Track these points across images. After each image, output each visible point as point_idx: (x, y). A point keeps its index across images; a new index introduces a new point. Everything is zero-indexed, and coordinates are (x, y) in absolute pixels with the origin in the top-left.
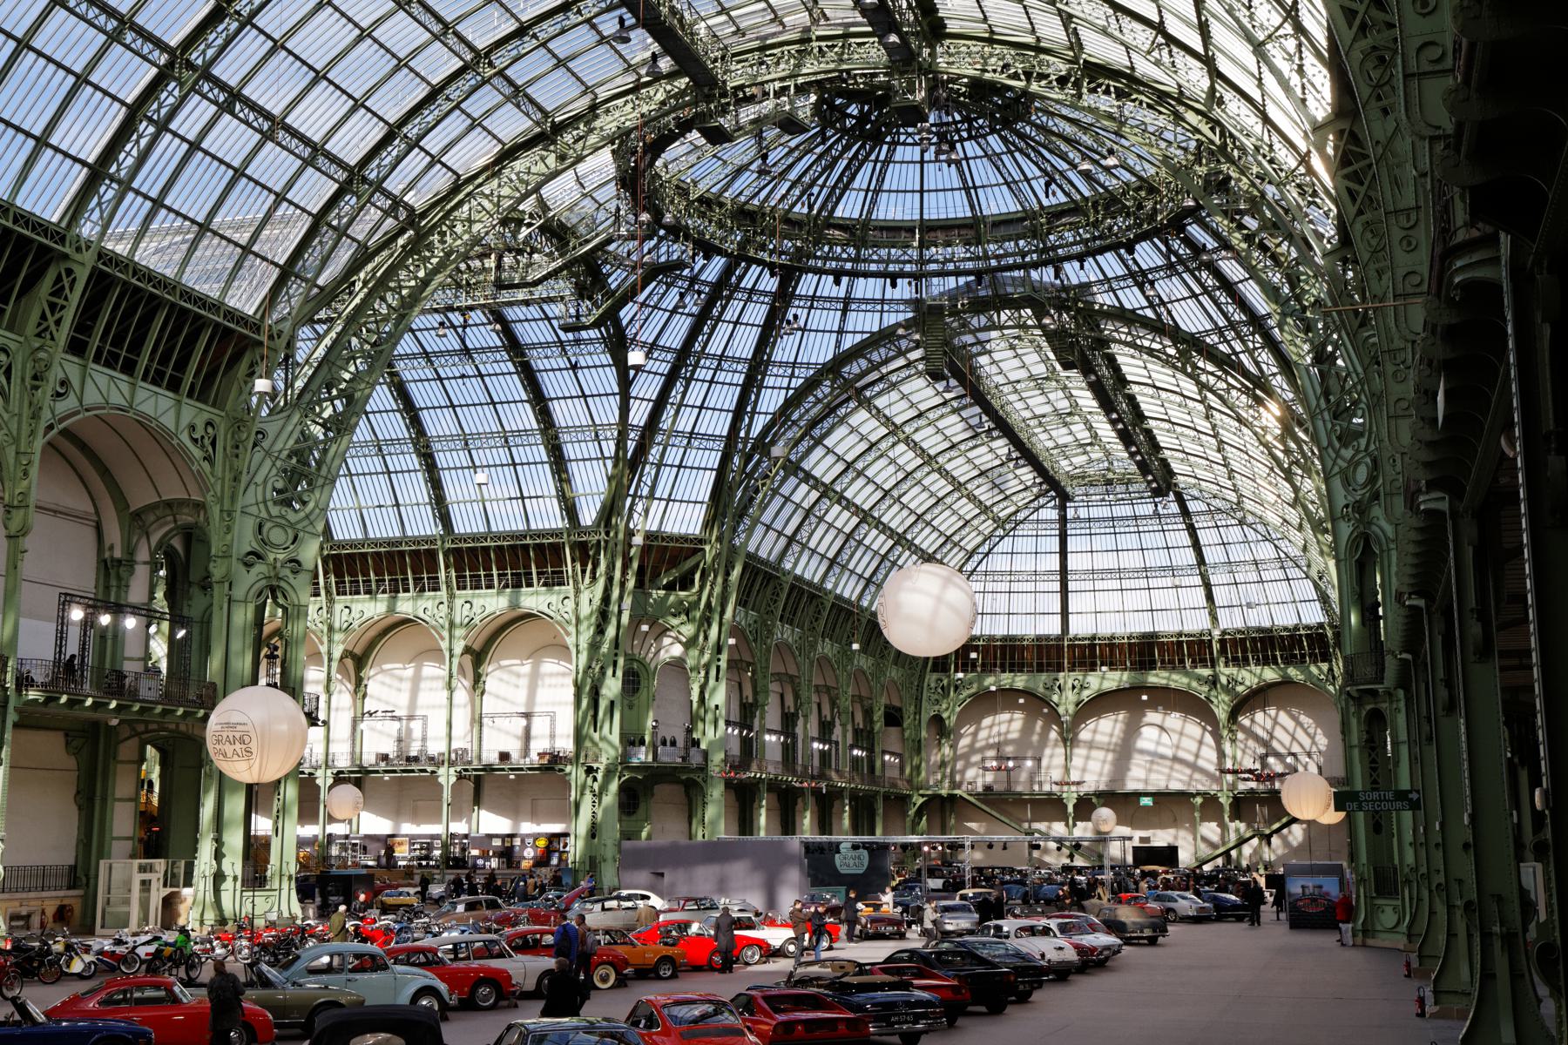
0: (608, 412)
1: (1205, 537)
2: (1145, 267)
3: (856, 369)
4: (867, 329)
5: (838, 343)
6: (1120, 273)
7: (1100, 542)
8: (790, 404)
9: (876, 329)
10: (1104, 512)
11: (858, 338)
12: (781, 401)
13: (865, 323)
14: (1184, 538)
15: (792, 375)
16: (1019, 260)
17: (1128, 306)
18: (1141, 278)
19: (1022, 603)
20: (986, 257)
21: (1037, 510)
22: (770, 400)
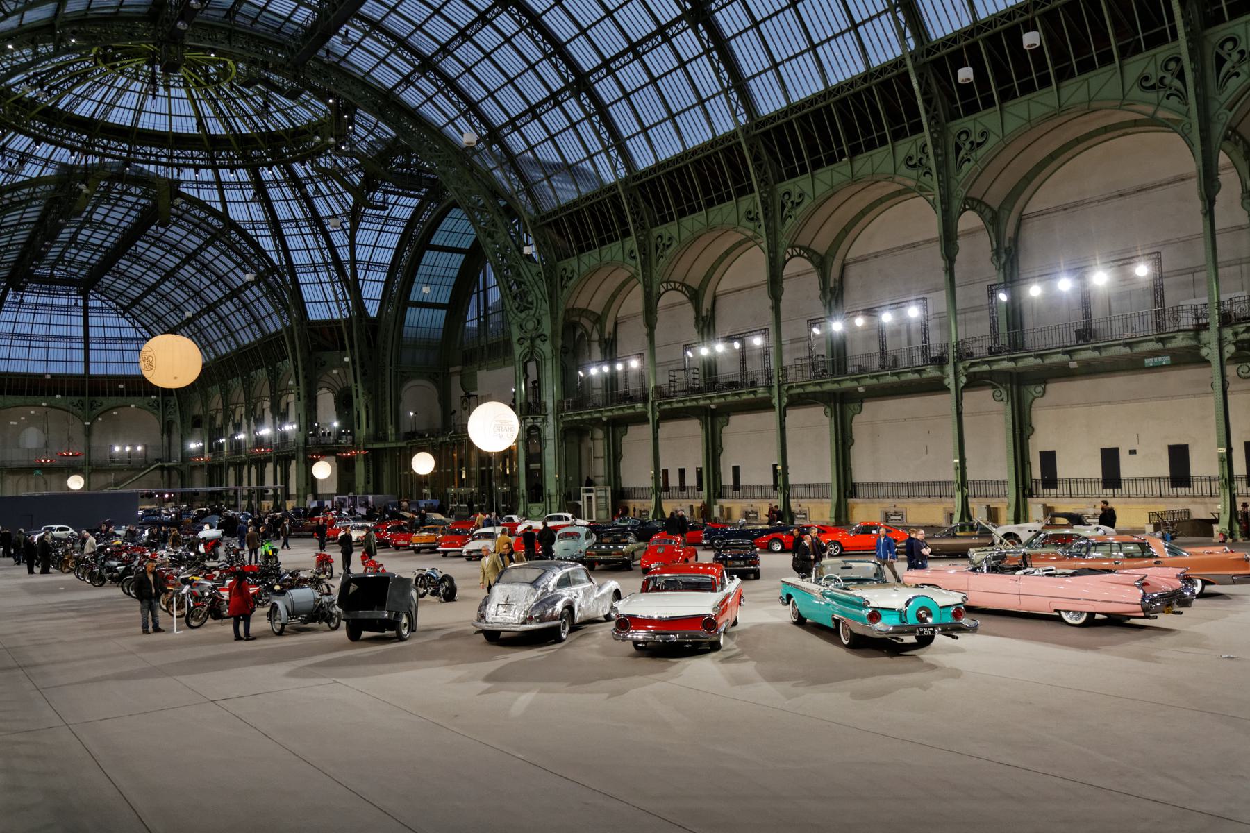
1: (92, 321)
3: (215, 223)
7: (26, 317)
9: (35, 176)
10: (49, 301)
13: (31, 170)
16: (191, 162)
18: (220, 185)
19: (38, 354)
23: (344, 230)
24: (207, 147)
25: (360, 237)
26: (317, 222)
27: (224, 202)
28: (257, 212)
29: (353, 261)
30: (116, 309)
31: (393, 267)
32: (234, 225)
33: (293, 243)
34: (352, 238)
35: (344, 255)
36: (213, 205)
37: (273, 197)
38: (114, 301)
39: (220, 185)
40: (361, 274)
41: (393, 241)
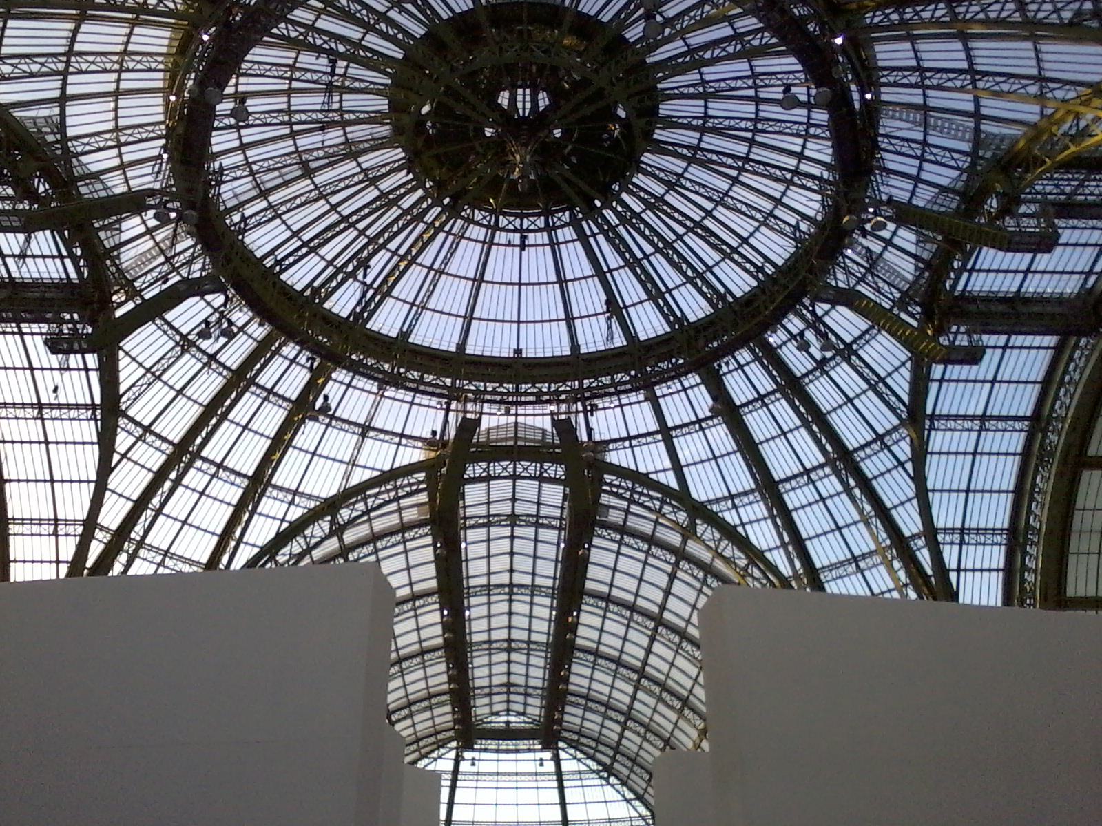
0: (76, 504)
2: (670, 424)
4: (378, 466)
5: (347, 476)
6: (643, 431)
7: (487, 796)
8: (282, 539)
9: (387, 468)
11: (367, 475)
12: (272, 535)
14: (554, 796)
15: (291, 503)
17: (642, 470)
18: (666, 433)
20: (517, 393)
21: (435, 759)
22: (261, 531)
23: (901, 464)
24: (637, 366)
25: (936, 472)
26: (843, 460)
27: (677, 468)
28: (740, 477)
29: (930, 532)
30: (597, 772)
31: (1015, 537)
32: (700, 511)
33: (808, 522)
34: (919, 478)
35: (909, 521)
36: (662, 478)
37: (758, 436)
38: (593, 758)
39: (666, 433)
40: (950, 555)
41: (1004, 473)
